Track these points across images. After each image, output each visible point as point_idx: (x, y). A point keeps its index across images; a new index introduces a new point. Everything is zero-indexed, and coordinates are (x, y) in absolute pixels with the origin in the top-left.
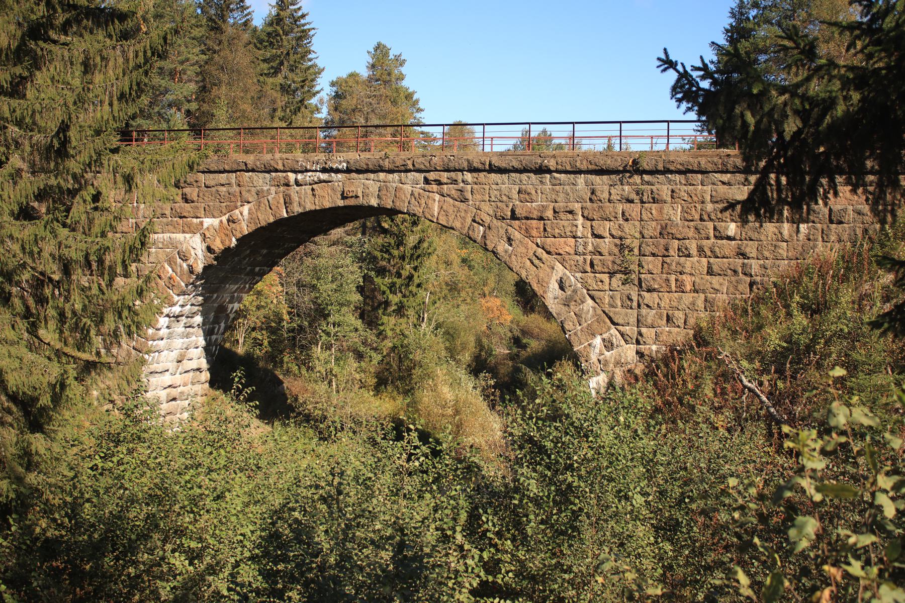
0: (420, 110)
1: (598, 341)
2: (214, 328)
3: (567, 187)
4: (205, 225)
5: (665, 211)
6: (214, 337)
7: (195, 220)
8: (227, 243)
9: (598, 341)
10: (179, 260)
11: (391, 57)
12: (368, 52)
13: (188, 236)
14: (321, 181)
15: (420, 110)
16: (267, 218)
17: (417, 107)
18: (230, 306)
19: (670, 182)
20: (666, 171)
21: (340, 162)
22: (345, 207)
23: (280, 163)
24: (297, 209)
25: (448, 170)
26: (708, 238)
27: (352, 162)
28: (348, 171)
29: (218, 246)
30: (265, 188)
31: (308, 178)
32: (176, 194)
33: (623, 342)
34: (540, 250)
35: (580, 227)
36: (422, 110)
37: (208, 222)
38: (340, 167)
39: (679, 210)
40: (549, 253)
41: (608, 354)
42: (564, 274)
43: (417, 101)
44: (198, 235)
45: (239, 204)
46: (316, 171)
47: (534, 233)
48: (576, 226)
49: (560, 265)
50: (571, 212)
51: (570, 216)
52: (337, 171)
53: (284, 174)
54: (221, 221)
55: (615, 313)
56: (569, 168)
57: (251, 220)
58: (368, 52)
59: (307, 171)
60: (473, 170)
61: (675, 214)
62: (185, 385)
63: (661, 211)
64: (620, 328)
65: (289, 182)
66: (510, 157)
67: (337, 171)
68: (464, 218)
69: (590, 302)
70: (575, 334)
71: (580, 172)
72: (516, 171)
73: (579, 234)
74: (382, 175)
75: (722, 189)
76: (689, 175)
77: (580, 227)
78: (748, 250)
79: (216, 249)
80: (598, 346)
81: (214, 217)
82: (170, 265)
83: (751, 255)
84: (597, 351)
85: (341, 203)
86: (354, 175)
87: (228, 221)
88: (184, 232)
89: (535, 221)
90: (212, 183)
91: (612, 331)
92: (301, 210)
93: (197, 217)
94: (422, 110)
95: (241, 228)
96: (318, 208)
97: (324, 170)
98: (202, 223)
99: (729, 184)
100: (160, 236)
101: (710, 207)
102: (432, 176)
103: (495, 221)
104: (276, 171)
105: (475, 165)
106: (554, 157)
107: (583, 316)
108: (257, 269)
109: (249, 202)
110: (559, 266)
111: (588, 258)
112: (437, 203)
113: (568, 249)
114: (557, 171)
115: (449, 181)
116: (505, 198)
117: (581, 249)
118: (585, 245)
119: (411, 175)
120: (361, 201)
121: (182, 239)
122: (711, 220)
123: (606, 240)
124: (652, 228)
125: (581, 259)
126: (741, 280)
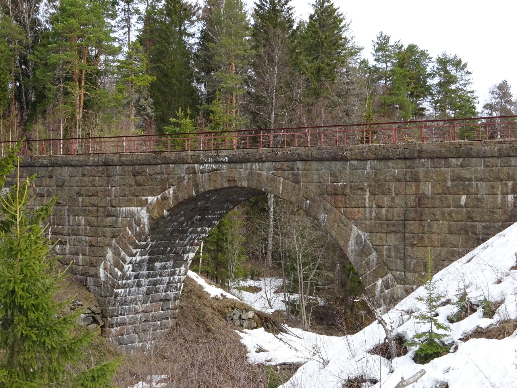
0: (468, 73)
1: (379, 282)
2: (175, 271)
3: (359, 171)
4: (149, 201)
5: (421, 187)
6: (176, 277)
7: (143, 198)
8: (161, 213)
9: (379, 282)
10: (134, 225)
11: (391, 43)
12: (373, 41)
13: (139, 208)
14: (214, 170)
15: (468, 73)
16: (183, 196)
17: (466, 70)
18: (186, 255)
19: (423, 166)
20: (420, 158)
21: (224, 157)
22: (230, 188)
23: (189, 158)
24: (202, 190)
25: (287, 161)
26: (449, 207)
27: (230, 156)
28: (230, 162)
29: (156, 214)
30: (182, 175)
31: (206, 168)
32: (131, 180)
33: (395, 283)
34: (343, 217)
35: (367, 200)
36: (470, 73)
37: (150, 199)
38: (224, 160)
39: (430, 186)
40: (348, 219)
41: (386, 291)
42: (359, 234)
43: (465, 66)
44: (145, 208)
45: (168, 186)
46: (211, 163)
47: (340, 205)
48: (365, 199)
49: (355, 227)
50: (362, 189)
51: (360, 192)
52: (223, 163)
53: (193, 165)
54: (158, 198)
55: (390, 261)
56: (359, 158)
57: (176, 197)
58: (373, 41)
59: (206, 163)
60: (302, 160)
61: (428, 189)
62: (156, 310)
63: (418, 187)
64: (394, 273)
65: (195, 171)
66: (324, 150)
67: (223, 163)
68: (298, 195)
69: (374, 254)
70: (366, 277)
71: (367, 160)
72: (328, 160)
73: (367, 205)
74: (249, 165)
75: (457, 170)
76: (436, 160)
77: (367, 200)
78: (473, 215)
79: (154, 217)
80: (380, 285)
81: (154, 196)
82: (129, 229)
83: (477, 219)
84: (379, 289)
85: (226, 185)
86: (233, 165)
87: (161, 197)
88: (137, 206)
89: (340, 196)
90: (152, 172)
91: (388, 275)
92: (203, 191)
93: (144, 196)
94: (470, 73)
95: (169, 203)
96: (212, 189)
97: (216, 162)
98: (147, 199)
99: (461, 166)
100: (124, 209)
101: (449, 184)
102: (278, 165)
103: (316, 197)
104: (188, 163)
105: (303, 157)
106: (351, 150)
107: (370, 264)
108: (199, 229)
109: (173, 185)
110: (355, 228)
111: (373, 222)
112: (281, 184)
113: (360, 216)
114: (352, 160)
115: (288, 169)
116: (321, 180)
117: (368, 215)
118: (371, 212)
119: (267, 165)
120: (239, 184)
121: (136, 211)
122: (450, 193)
123: (384, 209)
124: (412, 201)
125: (368, 222)
126: (470, 237)
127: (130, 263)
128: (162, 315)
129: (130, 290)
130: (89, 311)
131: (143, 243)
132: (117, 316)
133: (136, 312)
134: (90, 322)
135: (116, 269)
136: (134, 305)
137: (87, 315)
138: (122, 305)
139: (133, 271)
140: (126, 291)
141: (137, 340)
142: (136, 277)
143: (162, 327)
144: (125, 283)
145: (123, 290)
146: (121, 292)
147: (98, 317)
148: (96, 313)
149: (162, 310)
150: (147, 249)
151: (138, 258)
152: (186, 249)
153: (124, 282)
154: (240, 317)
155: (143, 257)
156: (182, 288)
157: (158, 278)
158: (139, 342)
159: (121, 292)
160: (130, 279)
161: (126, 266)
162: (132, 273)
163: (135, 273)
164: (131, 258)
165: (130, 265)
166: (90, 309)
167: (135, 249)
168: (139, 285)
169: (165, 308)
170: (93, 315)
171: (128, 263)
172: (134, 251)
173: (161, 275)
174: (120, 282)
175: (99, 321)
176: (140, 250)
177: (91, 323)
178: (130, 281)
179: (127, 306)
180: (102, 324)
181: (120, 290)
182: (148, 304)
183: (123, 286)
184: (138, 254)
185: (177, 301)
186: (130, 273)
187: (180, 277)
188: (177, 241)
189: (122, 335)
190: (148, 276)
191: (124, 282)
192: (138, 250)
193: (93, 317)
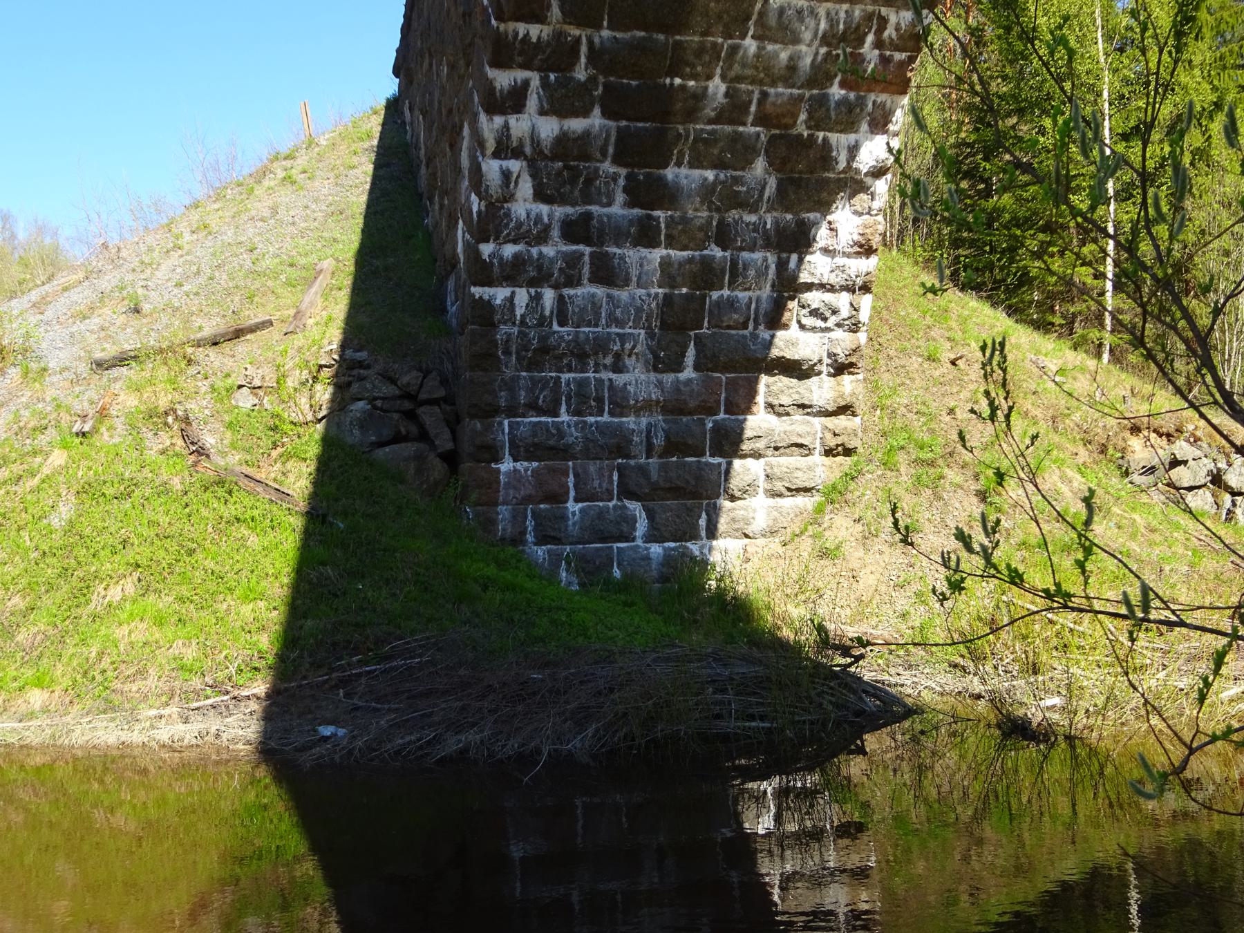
127: (505, 148)
128: (770, 432)
129: (561, 300)
130: (388, 390)
131: (535, 31)
132: (512, 412)
133: (620, 402)
134: (387, 433)
135: (473, 196)
136: (606, 375)
137: (379, 403)
138: (533, 365)
139: (540, 195)
140: (537, 298)
141: (642, 526)
142: (575, 230)
143: (779, 486)
144: (516, 256)
145: (522, 297)
146: (511, 300)
147: (430, 417)
148: (423, 396)
149: (770, 406)
150: (581, 73)
151: (549, 128)
152: (823, 100)
153: (509, 250)
154: (1217, 479)
155: (576, 125)
156: (864, 316)
157: (717, 252)
158: (651, 538)
159: (511, 300)
160: (542, 237)
161: (492, 168)
162: (544, 209)
163: (560, 211)
164: (498, 120)
165: (515, 165)
166: (393, 381)
167: (498, 64)
168: (607, 273)
169: (785, 400)
170: (407, 405)
171: (491, 145)
172: (503, 79)
173: (724, 237)
174: (486, 249)
175: (432, 432)
176: (535, 78)
177: (397, 439)
178: (549, 251)
179: (565, 376)
180: (444, 442)
181: (500, 294)
182: (688, 373)
183: (513, 273)
184: (532, 103)
185: (846, 379)
186: (524, 205)
187: (840, 261)
188: (750, 45)
189: (558, 498)
190: (646, 236)
191: (509, 250)
192: (521, 75)
193: (410, 415)
